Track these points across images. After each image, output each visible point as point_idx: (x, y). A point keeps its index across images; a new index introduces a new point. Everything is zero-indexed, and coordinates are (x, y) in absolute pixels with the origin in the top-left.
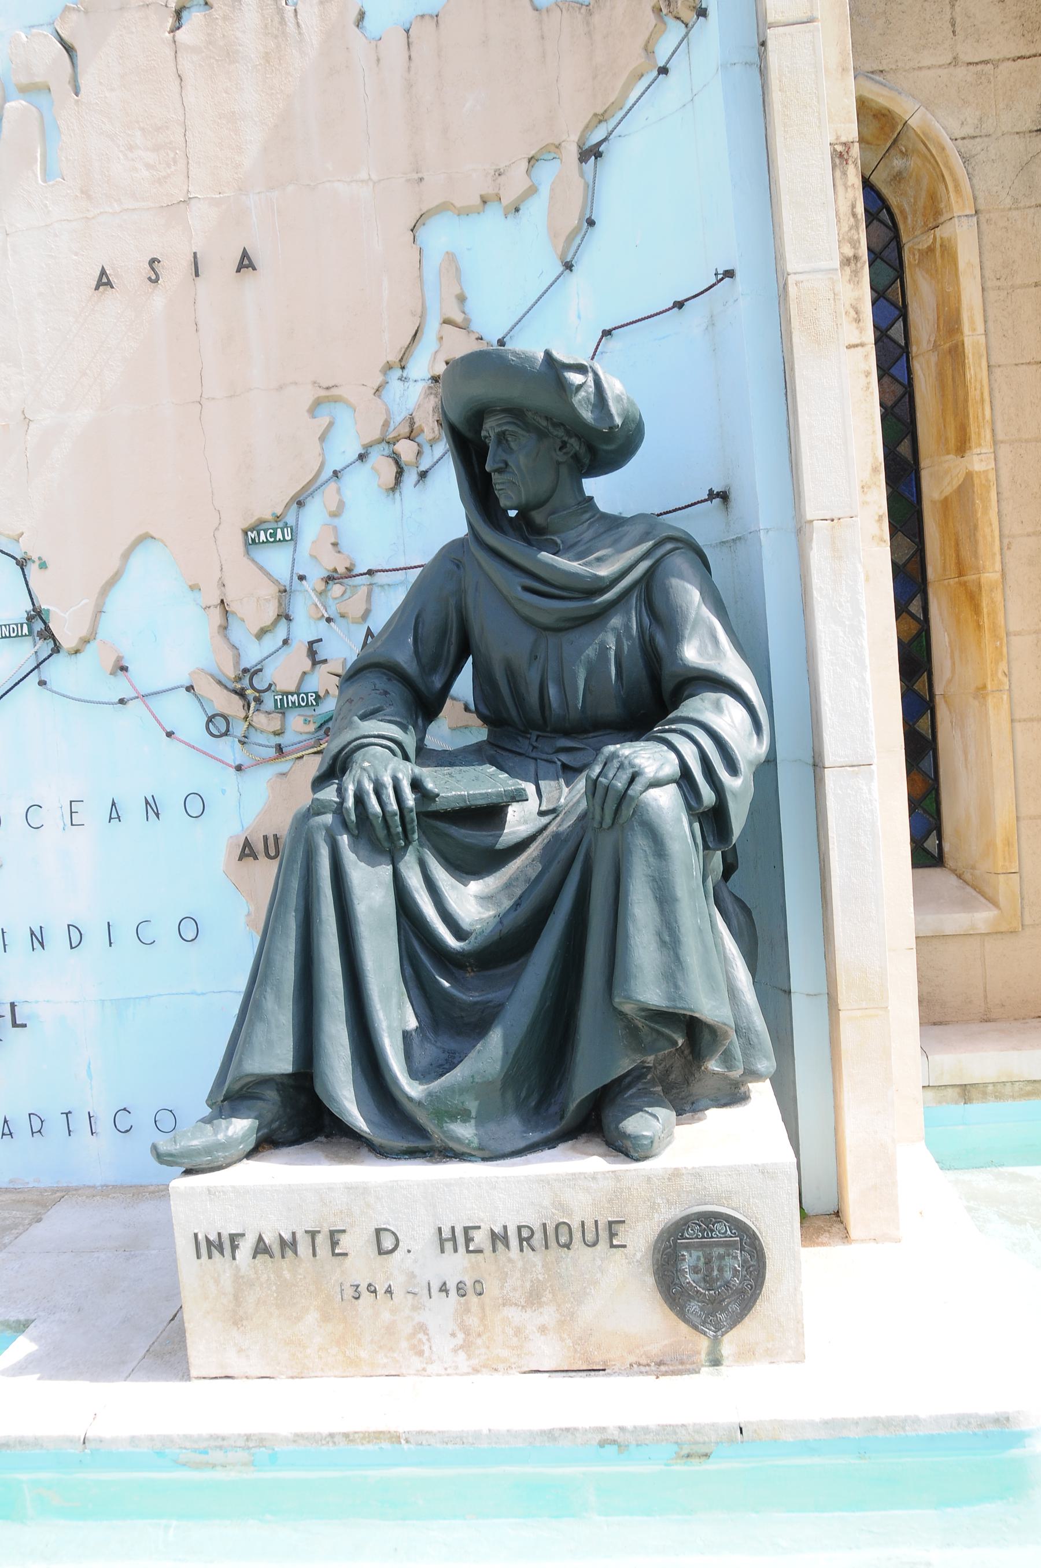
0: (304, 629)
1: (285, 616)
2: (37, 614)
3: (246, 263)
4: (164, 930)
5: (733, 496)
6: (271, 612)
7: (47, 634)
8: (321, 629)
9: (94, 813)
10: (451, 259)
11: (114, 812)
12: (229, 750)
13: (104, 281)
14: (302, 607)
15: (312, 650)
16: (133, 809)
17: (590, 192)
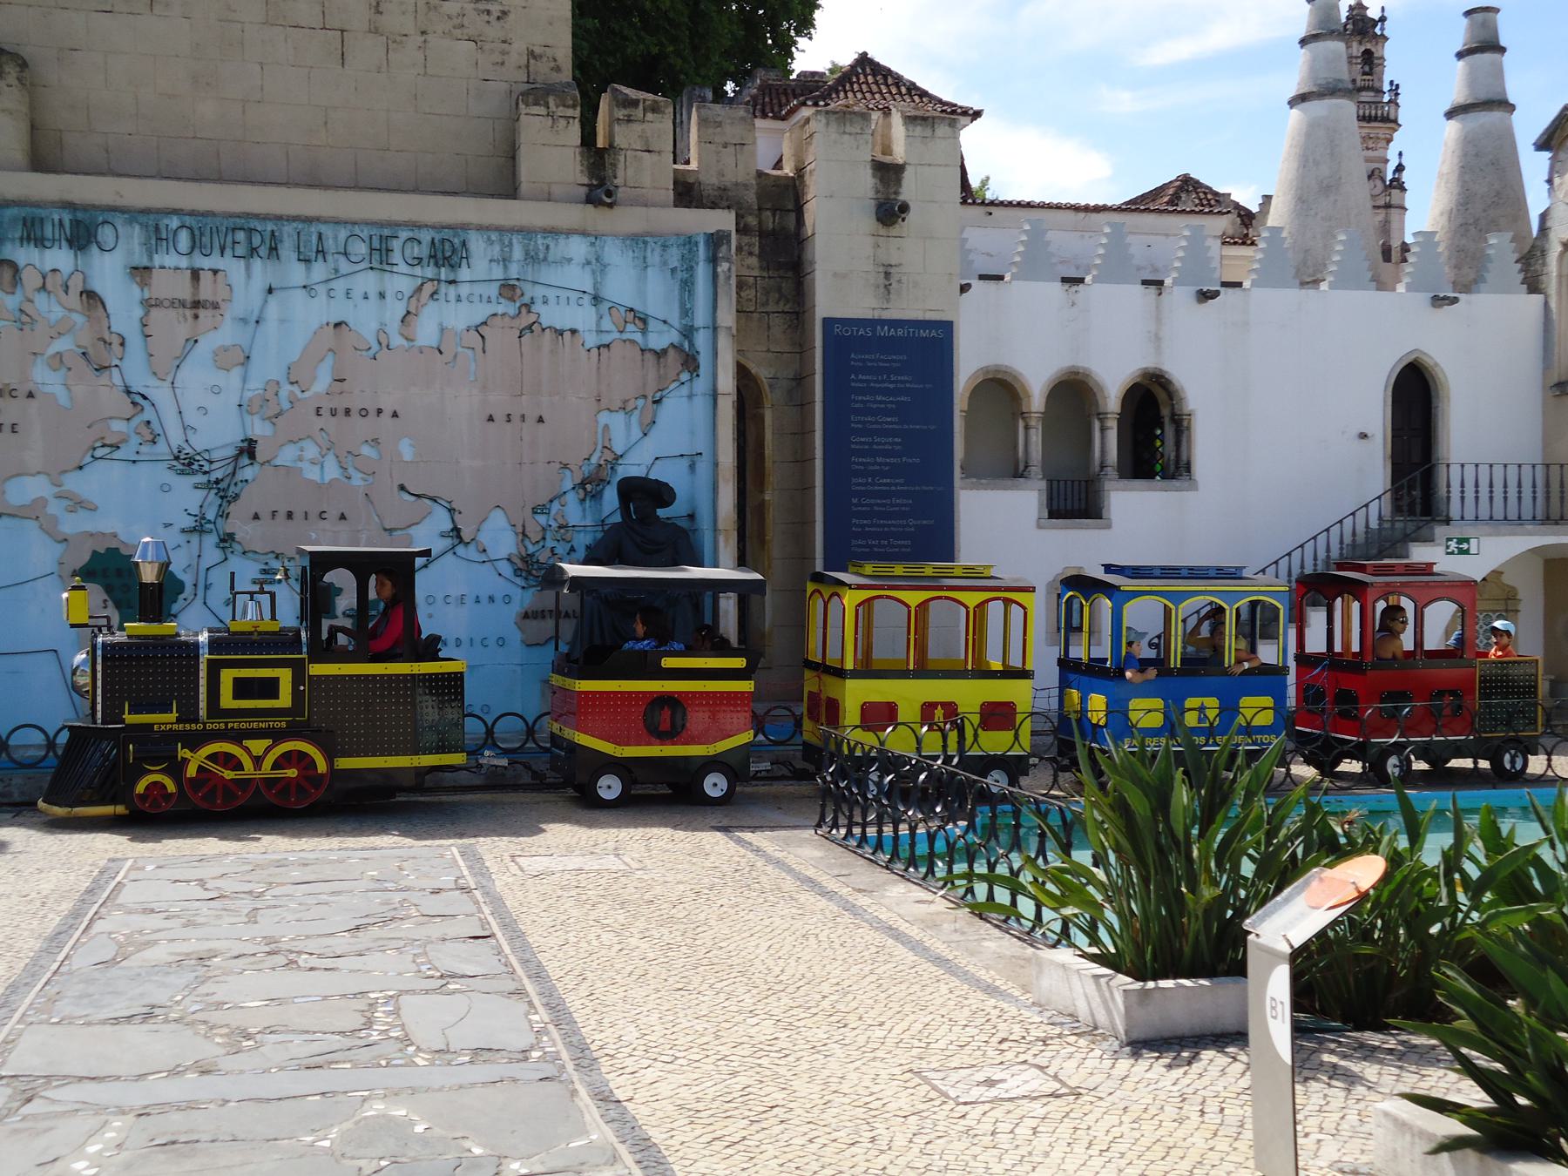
0: (550, 543)
1: (544, 539)
2: (456, 530)
3: (541, 420)
4: (492, 642)
5: (697, 516)
6: (540, 537)
7: (459, 537)
8: (554, 544)
9: (469, 601)
10: (606, 427)
11: (478, 601)
12: (519, 581)
13: (491, 419)
14: (548, 535)
15: (552, 549)
16: (484, 600)
17: (655, 415)
